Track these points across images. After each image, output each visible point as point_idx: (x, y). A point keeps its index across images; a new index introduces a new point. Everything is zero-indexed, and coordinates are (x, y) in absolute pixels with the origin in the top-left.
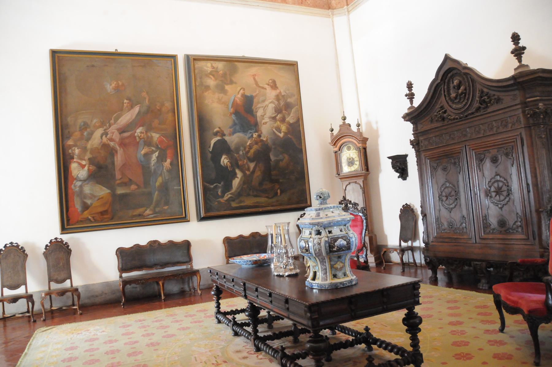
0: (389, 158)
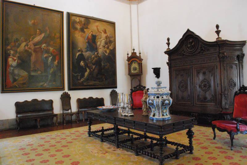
0: (153, 68)
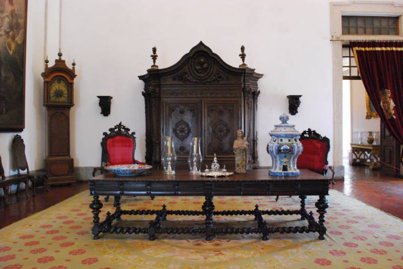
0: (98, 97)
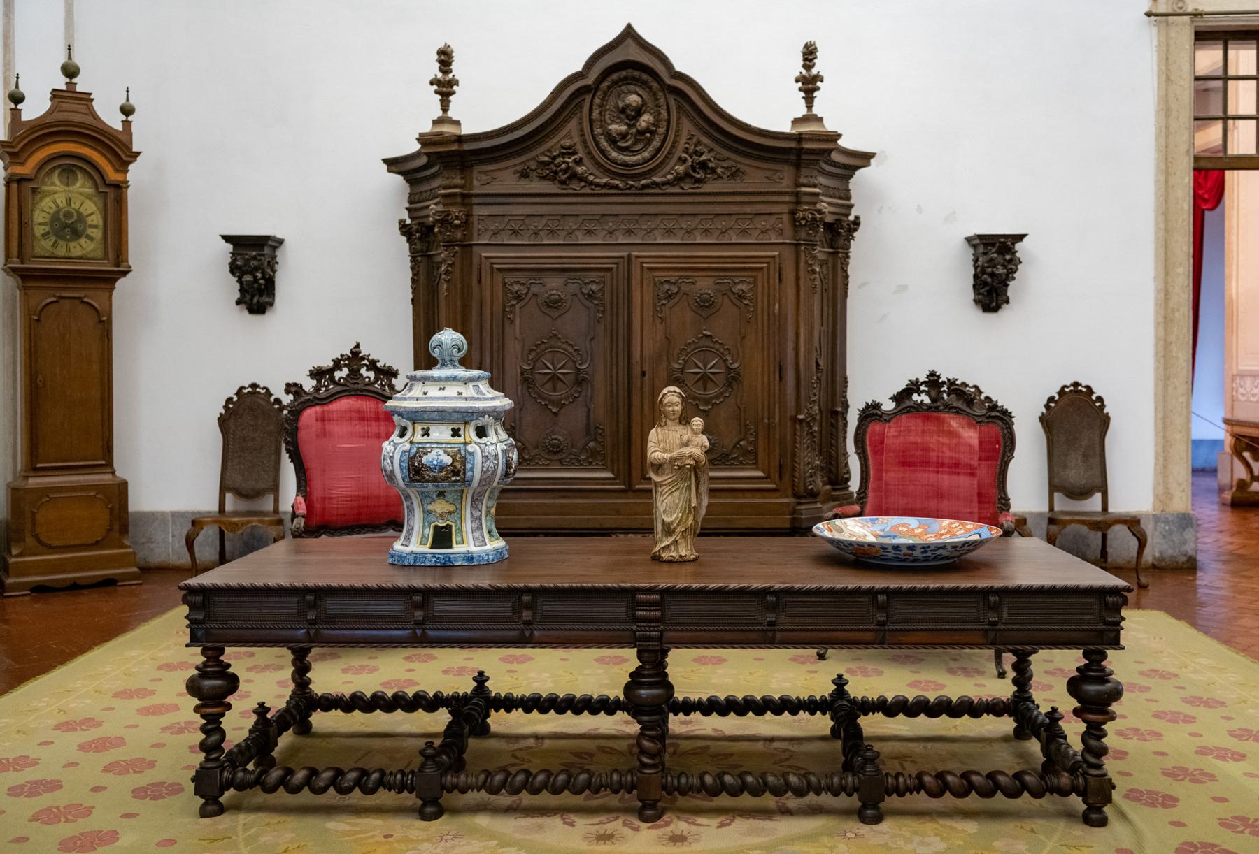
0: (227, 238)
